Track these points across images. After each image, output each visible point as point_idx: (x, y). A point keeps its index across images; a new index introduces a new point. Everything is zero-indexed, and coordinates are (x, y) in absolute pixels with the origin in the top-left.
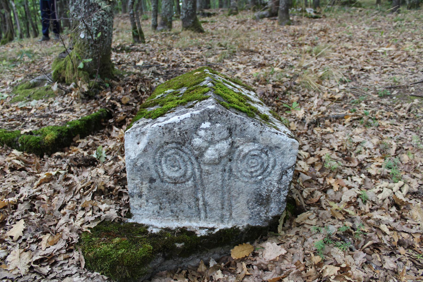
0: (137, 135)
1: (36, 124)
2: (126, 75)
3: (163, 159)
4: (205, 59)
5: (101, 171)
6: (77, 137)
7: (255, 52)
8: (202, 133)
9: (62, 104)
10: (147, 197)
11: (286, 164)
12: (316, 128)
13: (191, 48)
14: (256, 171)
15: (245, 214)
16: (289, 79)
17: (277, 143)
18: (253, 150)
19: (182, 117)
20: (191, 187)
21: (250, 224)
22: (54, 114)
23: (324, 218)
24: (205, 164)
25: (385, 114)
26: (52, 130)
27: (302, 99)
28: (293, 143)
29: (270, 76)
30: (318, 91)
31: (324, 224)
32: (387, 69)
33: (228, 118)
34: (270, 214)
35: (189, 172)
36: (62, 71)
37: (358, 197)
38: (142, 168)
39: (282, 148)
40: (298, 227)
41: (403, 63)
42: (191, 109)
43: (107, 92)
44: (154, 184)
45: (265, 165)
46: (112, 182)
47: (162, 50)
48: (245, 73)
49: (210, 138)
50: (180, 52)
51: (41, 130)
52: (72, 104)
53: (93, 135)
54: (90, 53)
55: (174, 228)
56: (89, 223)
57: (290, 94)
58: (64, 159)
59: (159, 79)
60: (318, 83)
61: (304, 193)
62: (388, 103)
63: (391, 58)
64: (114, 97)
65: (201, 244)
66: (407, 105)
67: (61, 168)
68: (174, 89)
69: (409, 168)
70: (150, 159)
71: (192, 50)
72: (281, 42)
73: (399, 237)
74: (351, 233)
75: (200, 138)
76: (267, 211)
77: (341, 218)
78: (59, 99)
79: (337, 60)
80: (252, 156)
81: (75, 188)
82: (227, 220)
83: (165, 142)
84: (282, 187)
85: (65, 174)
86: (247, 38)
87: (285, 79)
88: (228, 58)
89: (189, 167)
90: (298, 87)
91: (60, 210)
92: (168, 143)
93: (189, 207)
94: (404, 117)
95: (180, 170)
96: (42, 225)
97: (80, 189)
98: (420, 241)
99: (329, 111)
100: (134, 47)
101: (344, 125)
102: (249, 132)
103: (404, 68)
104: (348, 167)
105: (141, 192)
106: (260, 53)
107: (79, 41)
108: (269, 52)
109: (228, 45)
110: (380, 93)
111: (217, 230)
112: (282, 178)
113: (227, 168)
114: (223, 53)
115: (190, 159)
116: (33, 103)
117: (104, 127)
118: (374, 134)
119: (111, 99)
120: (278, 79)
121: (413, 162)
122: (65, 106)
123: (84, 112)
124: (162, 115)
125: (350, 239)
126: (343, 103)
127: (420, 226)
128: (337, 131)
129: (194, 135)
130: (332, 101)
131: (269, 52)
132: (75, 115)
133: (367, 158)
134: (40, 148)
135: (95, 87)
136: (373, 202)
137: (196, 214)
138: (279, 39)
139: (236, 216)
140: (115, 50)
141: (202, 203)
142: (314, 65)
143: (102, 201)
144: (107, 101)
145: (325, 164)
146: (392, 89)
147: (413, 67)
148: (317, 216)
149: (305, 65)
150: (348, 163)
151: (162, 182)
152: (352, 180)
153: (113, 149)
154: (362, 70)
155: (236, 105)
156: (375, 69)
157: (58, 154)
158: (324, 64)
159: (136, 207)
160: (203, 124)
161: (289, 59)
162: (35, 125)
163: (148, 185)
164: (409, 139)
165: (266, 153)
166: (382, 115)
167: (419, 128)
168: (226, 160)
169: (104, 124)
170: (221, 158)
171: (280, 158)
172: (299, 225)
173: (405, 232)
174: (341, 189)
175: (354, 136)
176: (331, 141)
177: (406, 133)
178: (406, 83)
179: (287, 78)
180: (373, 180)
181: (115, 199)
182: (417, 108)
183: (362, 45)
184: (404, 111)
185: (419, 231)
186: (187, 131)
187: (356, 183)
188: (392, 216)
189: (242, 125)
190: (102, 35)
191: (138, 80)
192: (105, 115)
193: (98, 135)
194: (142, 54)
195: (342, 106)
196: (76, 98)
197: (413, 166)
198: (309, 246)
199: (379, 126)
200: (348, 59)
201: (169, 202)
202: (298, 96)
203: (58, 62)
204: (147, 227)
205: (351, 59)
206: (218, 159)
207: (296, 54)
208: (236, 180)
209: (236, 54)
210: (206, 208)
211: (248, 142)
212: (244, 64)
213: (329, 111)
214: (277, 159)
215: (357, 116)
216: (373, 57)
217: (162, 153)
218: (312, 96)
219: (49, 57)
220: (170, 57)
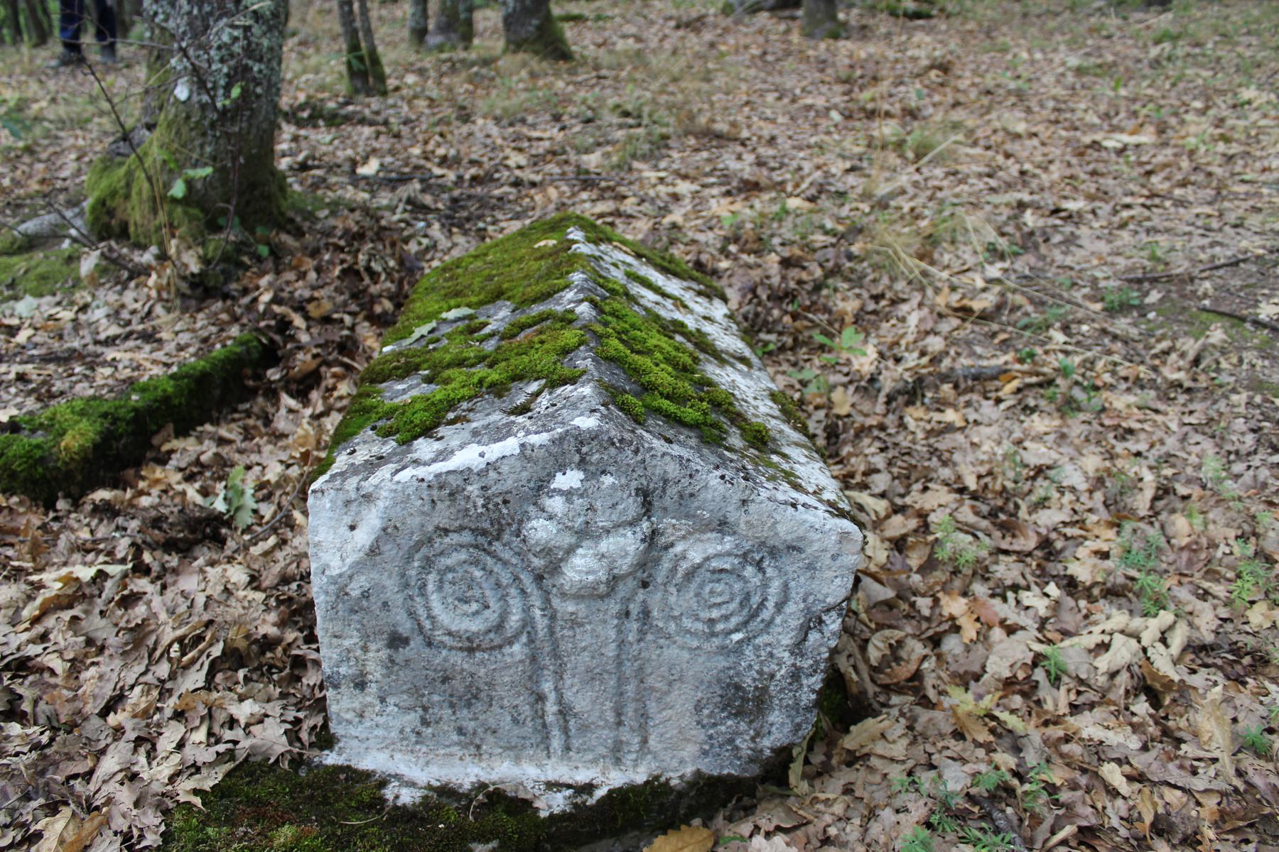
0: (348, 503)
1: (33, 390)
2: (322, 214)
3: (432, 578)
4: (573, 157)
5: (238, 575)
6: (163, 434)
7: (729, 139)
8: (556, 504)
9: (117, 312)
10: (380, 689)
11: (820, 597)
12: (910, 410)
13: (530, 119)
14: (726, 618)
15: (688, 740)
16: (834, 240)
17: (794, 536)
18: (716, 556)
19: (495, 450)
20: (521, 661)
21: (704, 769)
22: (91, 348)
23: (932, 732)
24: (564, 595)
25: (1122, 372)
26: (82, 413)
27: (871, 306)
28: (844, 536)
29: (775, 225)
30: (920, 284)
31: (930, 755)
32: (1132, 212)
33: (639, 458)
34: (766, 743)
35: (514, 619)
36: (118, 201)
37: (1035, 664)
38: (365, 603)
39: (809, 551)
40: (849, 764)
41: (1178, 192)
42: (520, 419)
43: (262, 274)
44: (403, 654)
45: (756, 600)
46: (273, 617)
47: (437, 124)
48: (696, 212)
49: (581, 519)
50: (495, 131)
51: (48, 413)
52: (149, 313)
53: (216, 423)
54: (208, 149)
55: (467, 786)
56: (198, 770)
57: (836, 290)
58: (120, 520)
59: (429, 225)
60: (921, 257)
61: (871, 648)
62: (1134, 332)
63: (1142, 170)
64: (285, 295)
65: (550, 838)
66: (1191, 346)
67: (110, 553)
68: (469, 306)
69: (1190, 563)
70: (390, 577)
71: (533, 126)
72: (809, 101)
73: (1155, 804)
74: (1010, 791)
75: (550, 518)
76: (758, 734)
77: (984, 736)
78: (109, 296)
79: (980, 176)
80: (714, 572)
81: (153, 638)
82: (634, 756)
84: (806, 663)
85: (125, 575)
86: (705, 87)
87: (819, 239)
88: (644, 158)
89: (515, 604)
90: (859, 267)
91: (104, 713)
92: (446, 531)
93: (515, 721)
94: (1181, 386)
95: (487, 613)
96: (42, 773)
97: (170, 645)
98: (1216, 817)
99: (952, 352)
100: (351, 108)
101: (998, 401)
103: (1181, 210)
104: (1006, 552)
105: (363, 674)
106: (743, 144)
107: (173, 110)
108: (772, 141)
109: (646, 110)
110: (1109, 298)
111: (600, 793)
112: (805, 639)
113: (634, 608)
114: (630, 138)
115: (516, 578)
116: (25, 306)
117: (251, 394)
118: (1087, 440)
119: (276, 300)
120: (797, 238)
121: (1204, 541)
122: (129, 323)
123: (188, 346)
124: (427, 431)
125: (1009, 810)
126: (995, 327)
127: (1218, 765)
128: (976, 422)
129: (531, 508)
130: (964, 320)
131: (772, 141)
132: (159, 355)
133: (1065, 524)
134: (43, 476)
135: (226, 258)
136: (1081, 682)
137: (536, 738)
138: (803, 90)
139: (660, 746)
140: (292, 116)
141: (555, 708)
142: (911, 191)
143: (240, 689)
144: (261, 308)
145: (937, 549)
146: (1146, 285)
147: (1207, 210)
148: (910, 728)
149: (882, 189)
150: (1008, 539)
151: (430, 644)
152: (1018, 602)
153: (278, 485)
154: (1056, 211)
155: (665, 404)
156: (1094, 212)
157: (102, 495)
158: (940, 189)
159: (349, 716)
160: (559, 475)
161: (833, 170)
162: (30, 393)
163: (384, 654)
164: (1193, 459)
165: (759, 565)
166: (1114, 373)
167: (1223, 424)
168: (631, 583)
169: (251, 383)
170: (614, 580)
171: (802, 579)
172: (853, 759)
173: (1175, 787)
174: (983, 637)
175: (1027, 444)
176: (957, 457)
177: (1184, 439)
178: (1186, 264)
179: (826, 233)
180: (1083, 603)
181: (278, 683)
182: (1217, 354)
183: (1057, 122)
184: (1181, 363)
185: (1216, 785)
186: (508, 497)
187: (1031, 612)
188: (1136, 728)
189: (685, 481)
190: (245, 91)
191: (360, 236)
192: (255, 355)
193: (234, 420)
194: (378, 134)
195: (994, 335)
196: (165, 295)
197: (1203, 556)
198: (882, 839)
199: (1104, 410)
200: (1014, 170)
201: (452, 706)
202: (858, 296)
203: (105, 169)
204: (383, 784)
205: (1023, 173)
206: (608, 582)
207: (857, 150)
208: (662, 641)
209: (671, 143)
210: (566, 721)
211: (703, 532)
212: (693, 180)
213: (952, 352)
214: (792, 584)
215: (1038, 374)
216: (1090, 167)
217: (427, 559)
218: (904, 301)
219: (79, 132)
220: (463, 149)
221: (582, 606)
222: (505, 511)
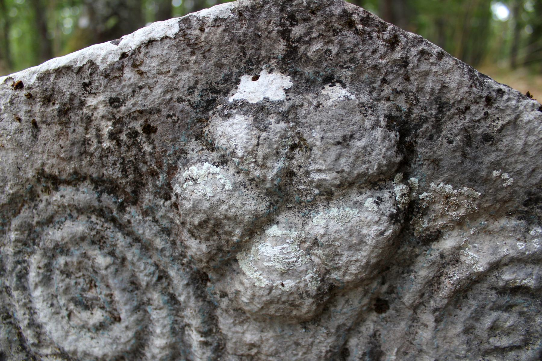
33: (397, 55)
49: (279, 165)
75: (223, 161)
80: (503, 291)
83: (41, 174)
95: (117, 329)
102: (509, 151)
115: (163, 276)
129: (193, 145)
160: (246, 81)
206: (319, 295)
211: (495, 216)
221: (269, 334)
222: (147, 148)
